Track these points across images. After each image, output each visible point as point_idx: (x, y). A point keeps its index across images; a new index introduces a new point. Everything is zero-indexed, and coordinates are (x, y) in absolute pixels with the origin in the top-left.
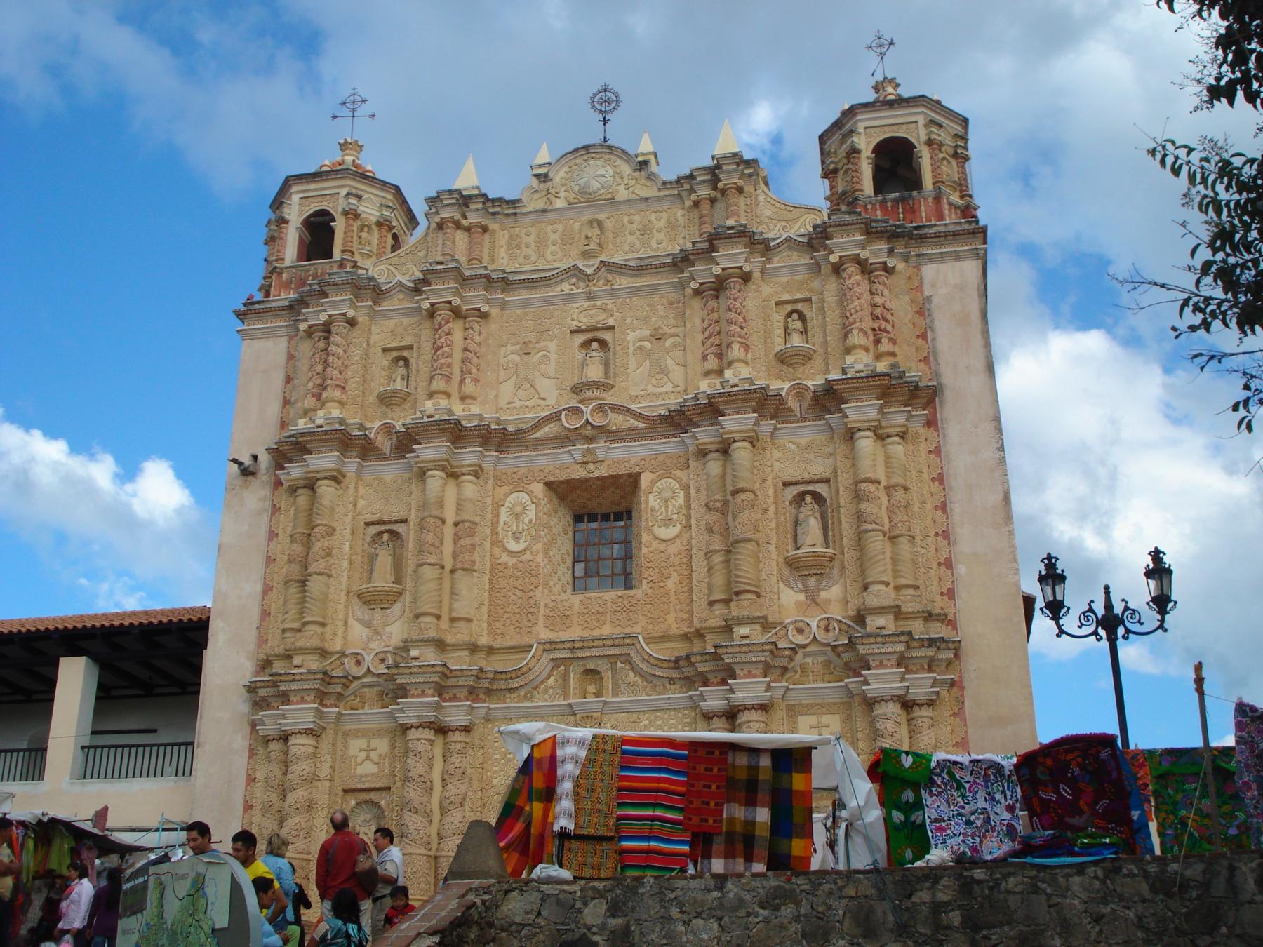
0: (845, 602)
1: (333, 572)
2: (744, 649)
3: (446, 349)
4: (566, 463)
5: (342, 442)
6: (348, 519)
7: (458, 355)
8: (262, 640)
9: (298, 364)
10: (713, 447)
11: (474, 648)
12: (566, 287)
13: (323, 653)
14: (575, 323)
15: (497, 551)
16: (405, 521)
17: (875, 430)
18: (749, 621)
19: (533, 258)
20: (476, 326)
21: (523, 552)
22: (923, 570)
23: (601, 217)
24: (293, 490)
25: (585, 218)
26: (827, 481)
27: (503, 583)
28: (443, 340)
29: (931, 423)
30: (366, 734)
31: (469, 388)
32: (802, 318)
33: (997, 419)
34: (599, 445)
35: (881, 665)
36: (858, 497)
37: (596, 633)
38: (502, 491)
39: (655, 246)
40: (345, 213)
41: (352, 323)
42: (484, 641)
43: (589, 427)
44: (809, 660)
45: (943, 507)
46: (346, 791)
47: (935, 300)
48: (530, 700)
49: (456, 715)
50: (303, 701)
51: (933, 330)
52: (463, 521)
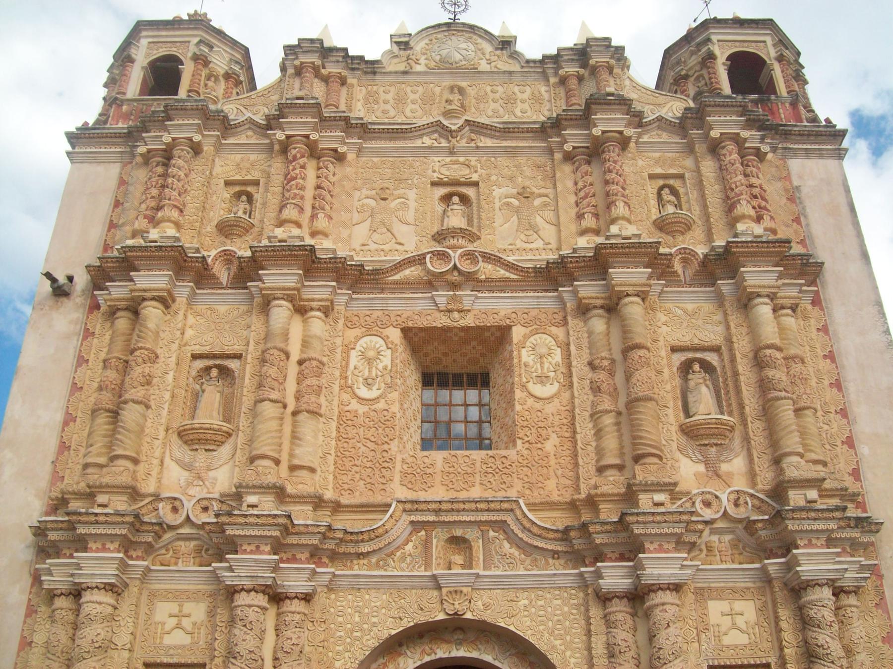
0: (752, 476)
1: (152, 403)
2: (658, 518)
3: (301, 181)
4: (426, 310)
5: (175, 260)
6: (175, 347)
7: (309, 193)
8: (56, 477)
9: (131, 188)
10: (599, 302)
11: (318, 502)
12: (427, 141)
13: (134, 494)
14: (435, 175)
15: (346, 397)
16: (238, 356)
17: (772, 297)
18: (659, 487)
19: (392, 113)
20: (331, 166)
21: (376, 400)
22: (827, 447)
23: (464, 84)
24: (112, 313)
25: (446, 84)
26: (716, 349)
27: (352, 432)
28: (297, 171)
29: (816, 302)
30: (179, 596)
31: (322, 223)
32: (674, 192)
33: (879, 304)
34: (465, 293)
35: (810, 545)
36: (759, 363)
37: (463, 495)
38: (351, 334)
39: (519, 114)
40: (196, 58)
41: (196, 149)
42: (329, 495)
43: (456, 273)
44: (715, 538)
45: (838, 385)
47: (805, 191)
48: (382, 568)
49: (295, 580)
50: (104, 549)
51: (805, 217)
52: (310, 359)
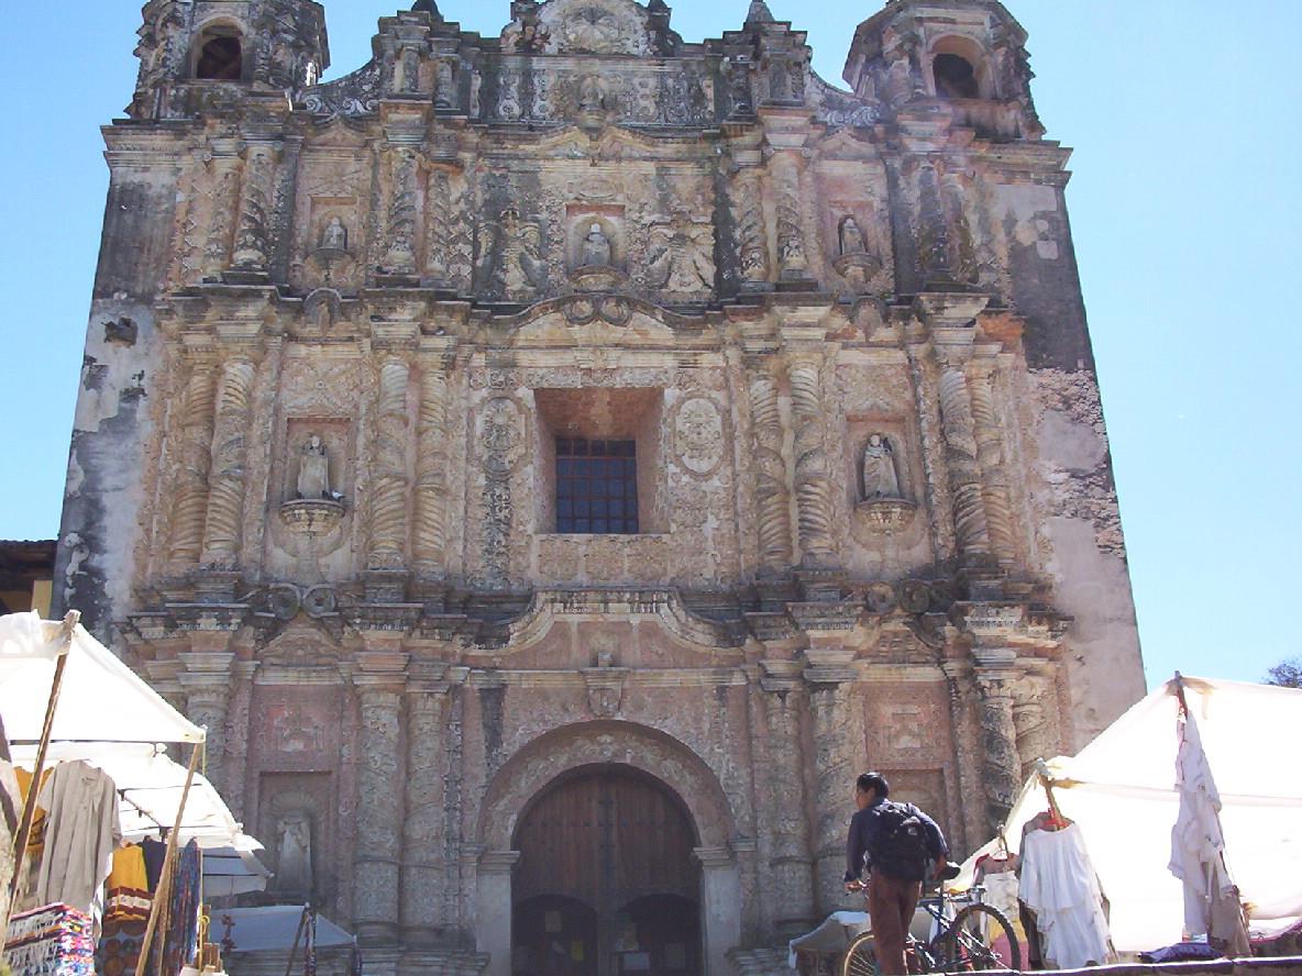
46: (262, 774)
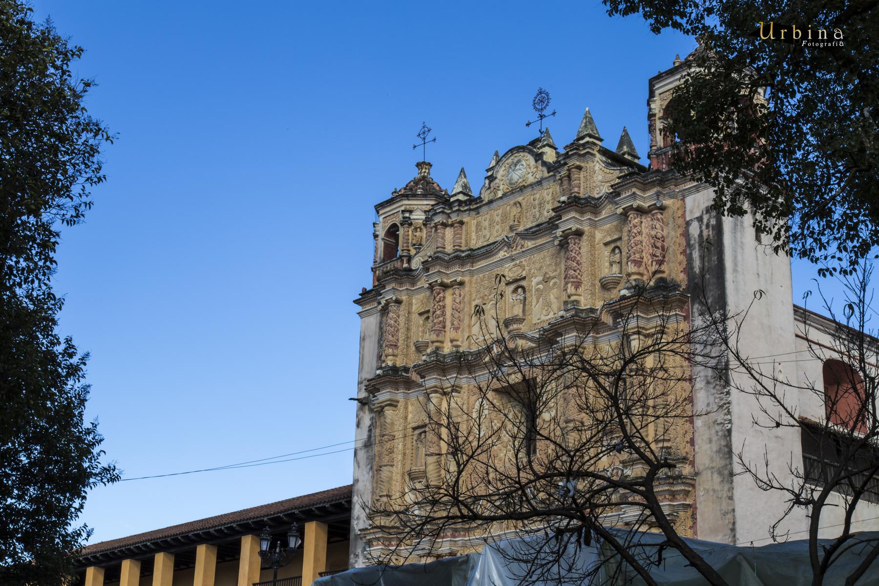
23: (520, 199)
25: (512, 202)
